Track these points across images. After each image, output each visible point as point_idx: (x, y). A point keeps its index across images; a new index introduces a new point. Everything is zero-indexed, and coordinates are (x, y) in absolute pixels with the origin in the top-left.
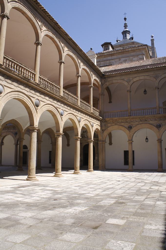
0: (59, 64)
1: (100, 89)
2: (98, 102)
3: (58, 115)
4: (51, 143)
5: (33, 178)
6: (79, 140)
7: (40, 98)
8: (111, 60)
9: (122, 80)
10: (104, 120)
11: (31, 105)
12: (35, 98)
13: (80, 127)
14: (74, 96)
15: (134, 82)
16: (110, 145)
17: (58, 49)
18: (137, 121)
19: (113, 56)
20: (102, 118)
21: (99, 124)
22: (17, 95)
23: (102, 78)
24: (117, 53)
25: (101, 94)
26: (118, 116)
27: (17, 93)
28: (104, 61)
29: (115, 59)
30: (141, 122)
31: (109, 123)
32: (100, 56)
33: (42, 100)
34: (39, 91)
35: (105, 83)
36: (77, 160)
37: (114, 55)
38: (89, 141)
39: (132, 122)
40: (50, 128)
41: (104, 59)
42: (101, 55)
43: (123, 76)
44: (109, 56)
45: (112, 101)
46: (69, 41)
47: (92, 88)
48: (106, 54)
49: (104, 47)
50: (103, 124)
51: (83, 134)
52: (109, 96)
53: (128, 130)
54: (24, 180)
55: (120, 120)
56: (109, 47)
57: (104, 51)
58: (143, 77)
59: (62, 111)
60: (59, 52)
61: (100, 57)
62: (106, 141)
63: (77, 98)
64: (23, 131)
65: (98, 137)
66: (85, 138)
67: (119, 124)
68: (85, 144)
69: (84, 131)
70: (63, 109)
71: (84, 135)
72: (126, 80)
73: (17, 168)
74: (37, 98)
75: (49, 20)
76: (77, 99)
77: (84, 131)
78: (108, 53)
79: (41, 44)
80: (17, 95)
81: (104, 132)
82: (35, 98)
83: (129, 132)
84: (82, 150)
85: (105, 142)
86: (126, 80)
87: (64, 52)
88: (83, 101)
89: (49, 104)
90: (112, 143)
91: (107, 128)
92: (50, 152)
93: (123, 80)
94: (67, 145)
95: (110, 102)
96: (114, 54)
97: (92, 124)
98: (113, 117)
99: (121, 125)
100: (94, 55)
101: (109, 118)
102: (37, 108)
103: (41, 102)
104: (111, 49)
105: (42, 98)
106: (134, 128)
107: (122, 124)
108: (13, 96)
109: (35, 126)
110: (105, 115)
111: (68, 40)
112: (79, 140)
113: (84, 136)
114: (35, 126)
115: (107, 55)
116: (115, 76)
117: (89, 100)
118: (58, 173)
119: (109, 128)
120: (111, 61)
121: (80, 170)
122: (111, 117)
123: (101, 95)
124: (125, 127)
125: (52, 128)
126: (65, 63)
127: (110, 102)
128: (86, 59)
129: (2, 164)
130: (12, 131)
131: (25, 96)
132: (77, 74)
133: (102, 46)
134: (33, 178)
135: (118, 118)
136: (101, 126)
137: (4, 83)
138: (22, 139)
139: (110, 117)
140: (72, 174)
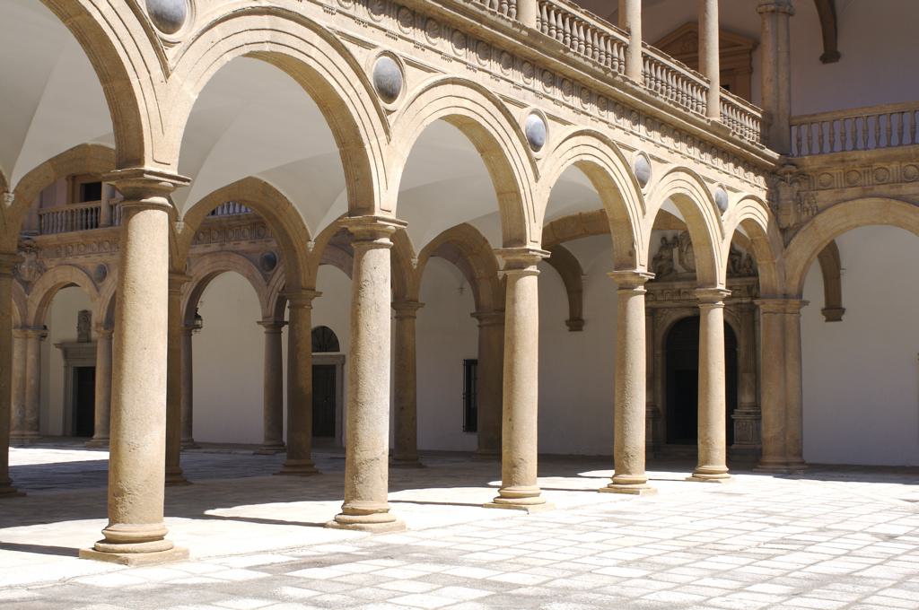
2: (751, 59)
3: (509, 144)
4: (472, 315)
5: (376, 512)
6: (641, 288)
7: (400, 48)
10: (794, 169)
11: (351, 92)
12: (374, 47)
13: (644, 213)
14: (606, 29)
16: (828, 320)
20: (776, 156)
21: (763, 196)
22: (267, 36)
25: (773, 7)
26: (883, 142)
27: (266, 21)
31: (825, 187)
33: (414, 58)
36: (628, 409)
38: (701, 294)
40: (464, 224)
45: (839, 49)
50: (786, 192)
51: (666, 254)
52: (822, 18)
54: (323, 525)
55: (894, 166)
59: (535, 119)
62: (805, 298)
63: (626, 36)
64: (311, 245)
65: (756, 274)
66: (678, 279)
67: (884, 189)
68: (675, 316)
69: (670, 238)
70: (542, 109)
71: (671, 260)
73: (282, 457)
74: (387, 48)
76: (621, 44)
77: (670, 238)
80: (267, 36)
81: (793, 243)
82: (374, 47)
84: (659, 352)
85: (797, 302)
88: (662, 56)
89: (455, 81)
90: (843, 311)
91: (814, 216)
92: (470, 365)
94: (568, 323)
95: (831, 55)
97: (717, 196)
98: (849, 144)
99: (898, 198)
101: (822, 152)
102: (390, 107)
103: (408, 69)
105: (418, 46)
108: (248, 37)
109: (377, 214)
110: (799, 140)
112: (640, 293)
113: (671, 270)
114: (377, 214)
117: (697, 51)
118: (519, 484)
119: (819, 219)
121: (646, 470)
122: (838, 146)
123: (773, 11)
125: (473, 225)
127: (831, 55)
129: (196, 436)
130: (244, 245)
131: (317, 40)
134: (376, 512)
135: (883, 152)
136: (774, 205)
138: (304, 292)
139: (827, 148)
140: (598, 491)
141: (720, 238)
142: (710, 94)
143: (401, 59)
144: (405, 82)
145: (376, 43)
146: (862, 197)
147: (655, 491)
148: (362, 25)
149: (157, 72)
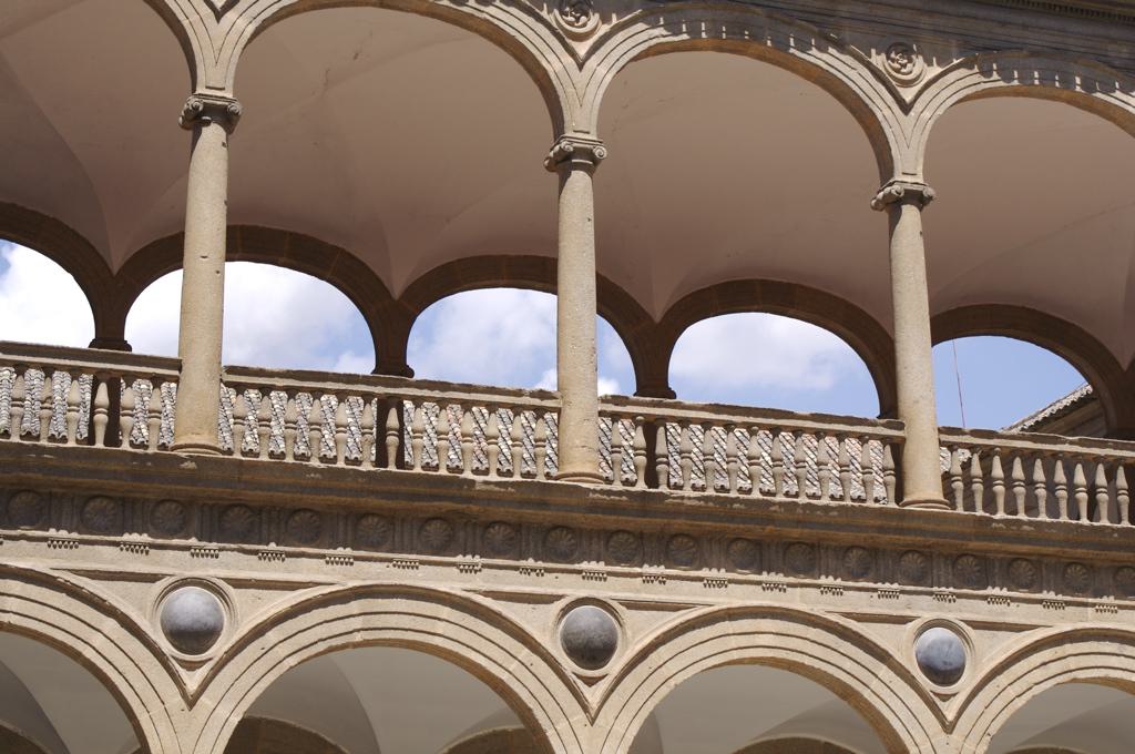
0: (884, 216)
3: (874, 683)
7: (612, 590)
11: (513, 666)
12: (559, 597)
17: (838, 96)
22: (357, 623)
34: (606, 531)
74: (583, 594)
79: (589, 154)
80: (357, 623)
82: (559, 597)
87: (906, 108)
126: (929, 191)
131: (445, 612)
137: (227, 566)
143: (615, 604)
144: (624, 633)
145: (560, 592)
148: (533, 574)
149: (174, 699)
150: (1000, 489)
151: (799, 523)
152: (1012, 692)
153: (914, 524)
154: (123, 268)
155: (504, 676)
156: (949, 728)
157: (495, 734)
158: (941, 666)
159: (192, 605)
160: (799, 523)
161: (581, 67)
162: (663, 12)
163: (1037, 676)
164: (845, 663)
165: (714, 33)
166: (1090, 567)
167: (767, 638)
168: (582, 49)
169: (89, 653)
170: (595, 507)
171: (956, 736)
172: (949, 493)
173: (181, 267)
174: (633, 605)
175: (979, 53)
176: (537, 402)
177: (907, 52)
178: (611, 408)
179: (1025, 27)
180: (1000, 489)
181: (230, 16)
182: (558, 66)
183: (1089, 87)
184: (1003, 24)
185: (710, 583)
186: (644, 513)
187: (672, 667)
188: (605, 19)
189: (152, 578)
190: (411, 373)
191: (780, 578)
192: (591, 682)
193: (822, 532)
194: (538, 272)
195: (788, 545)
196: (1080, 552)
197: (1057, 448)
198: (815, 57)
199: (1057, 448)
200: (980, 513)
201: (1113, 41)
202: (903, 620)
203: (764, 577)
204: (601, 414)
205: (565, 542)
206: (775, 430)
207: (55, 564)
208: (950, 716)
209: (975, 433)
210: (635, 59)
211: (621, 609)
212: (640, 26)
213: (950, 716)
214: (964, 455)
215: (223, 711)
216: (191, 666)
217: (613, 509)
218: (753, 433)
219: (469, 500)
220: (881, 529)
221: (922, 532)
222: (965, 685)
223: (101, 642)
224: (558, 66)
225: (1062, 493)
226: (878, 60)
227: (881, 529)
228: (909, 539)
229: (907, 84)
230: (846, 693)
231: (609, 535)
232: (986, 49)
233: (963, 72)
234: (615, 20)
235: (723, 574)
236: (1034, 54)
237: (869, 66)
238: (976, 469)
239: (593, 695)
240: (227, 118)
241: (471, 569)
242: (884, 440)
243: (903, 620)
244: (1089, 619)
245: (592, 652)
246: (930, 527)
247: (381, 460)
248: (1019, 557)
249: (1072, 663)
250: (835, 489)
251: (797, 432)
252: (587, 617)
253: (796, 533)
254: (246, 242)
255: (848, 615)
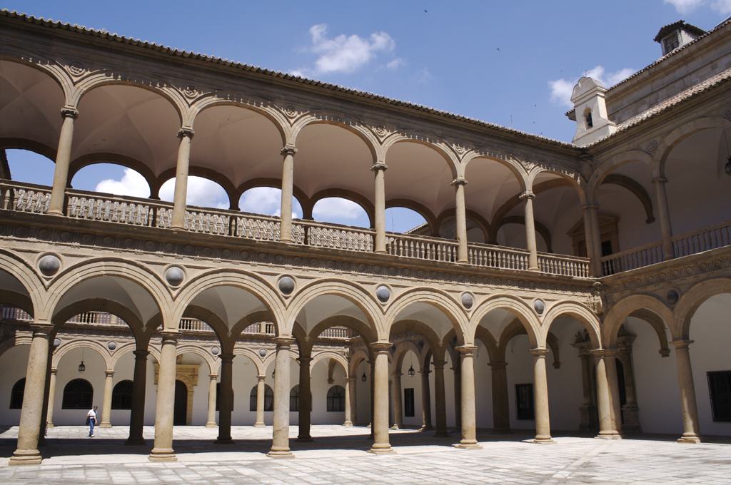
0: (374, 173)
1: (582, 193)
2: (617, 227)
8: (689, 77)
9: (634, 152)
11: (265, 293)
15: (669, 149)
16: (663, 356)
18: (690, 275)
19: (689, 62)
22: (222, 279)
23: (581, 159)
24: (700, 49)
25: (585, 207)
28: (668, 85)
29: (697, 70)
30: (702, 276)
31: (616, 291)
32: (652, 75)
35: (593, 171)
37: (694, 56)
39: (676, 278)
41: (667, 79)
42: (653, 70)
43: (636, 138)
44: (679, 67)
46: (397, 107)
47: (530, 202)
48: (666, 64)
49: (662, 41)
53: (666, 305)
55: (642, 277)
56: (679, 36)
57: (667, 53)
58: (692, 123)
60: (369, 146)
61: (653, 79)
63: (457, 242)
67: (639, 290)
72: (644, 147)
73: (434, 432)
74: (285, 274)
75: (313, 87)
78: (671, 60)
79: (293, 151)
80: (222, 279)
83: (670, 312)
86: (644, 147)
87: (381, 143)
91: (613, 306)
93: (638, 149)
96: (691, 54)
99: (646, 294)
100: (595, 89)
104: (685, 39)
106: (684, 297)
107: (650, 288)
111: (394, 107)
115: (672, 64)
116: (615, 145)
120: (685, 79)
124: (658, 298)
126: (386, 167)
128: (484, 128)
131: (246, 277)
132: (454, 179)
133: (658, 39)
137: (185, 261)
141: (539, 325)
142: (531, 257)
146: (631, 294)
147: (481, 448)
149: (169, 298)
150: (401, 249)
151: (346, 256)
152: (402, 304)
153: (379, 258)
154: (159, 176)
155: (262, 296)
156: (384, 314)
157: (259, 312)
158: (383, 296)
159: (175, 272)
160: (346, 256)
161: (291, 126)
162: (315, 112)
163: (408, 301)
164: (357, 295)
165: (329, 119)
166: (424, 271)
167: (336, 288)
168: (292, 121)
169: (145, 285)
170: (290, 250)
171: (386, 316)
172: (388, 250)
173: (175, 176)
174: (299, 277)
175: (402, 130)
176: (275, 219)
177: (382, 128)
178: (295, 222)
179: (414, 123)
180: (401, 249)
181: (193, 106)
182: (285, 126)
183: (430, 141)
184: (409, 122)
185: (321, 272)
186: (303, 251)
187: (309, 295)
188: (299, 113)
189: (164, 264)
190: (240, 210)
191: (341, 271)
192: (286, 298)
193: (352, 259)
194: (276, 183)
195: (343, 262)
196: (422, 267)
197: (417, 238)
198: (357, 127)
199: (417, 238)
200: (396, 255)
201: (437, 129)
202: (373, 284)
203: (336, 270)
204: (293, 223)
205: (281, 259)
206: (341, 230)
207: (137, 259)
208: (385, 311)
209: (396, 234)
210: (307, 125)
211: (296, 278)
212: (309, 116)
213: (385, 311)
214: (392, 239)
215: (183, 303)
216: (174, 289)
217: (294, 250)
218: (335, 231)
219: (254, 246)
220: (369, 259)
221: (379, 260)
222: (389, 302)
223: (149, 282)
224: (285, 126)
225: (418, 251)
226: (374, 130)
227: (369, 259)
228: (376, 262)
229: (382, 137)
230: (357, 304)
231: (293, 257)
232: (404, 129)
233: (397, 134)
234: (302, 114)
235: (324, 269)
236: (417, 131)
237: (371, 131)
238: (395, 243)
239: (287, 302)
240: (190, 135)
241: (254, 265)
242: (371, 234)
243: (373, 284)
244: (423, 285)
245: (287, 290)
246: (382, 258)
247: (230, 234)
248: (405, 268)
249: (418, 297)
250: (357, 247)
251: (347, 231)
252: (286, 280)
253: (345, 259)
254: (195, 170)
255: (358, 282)
